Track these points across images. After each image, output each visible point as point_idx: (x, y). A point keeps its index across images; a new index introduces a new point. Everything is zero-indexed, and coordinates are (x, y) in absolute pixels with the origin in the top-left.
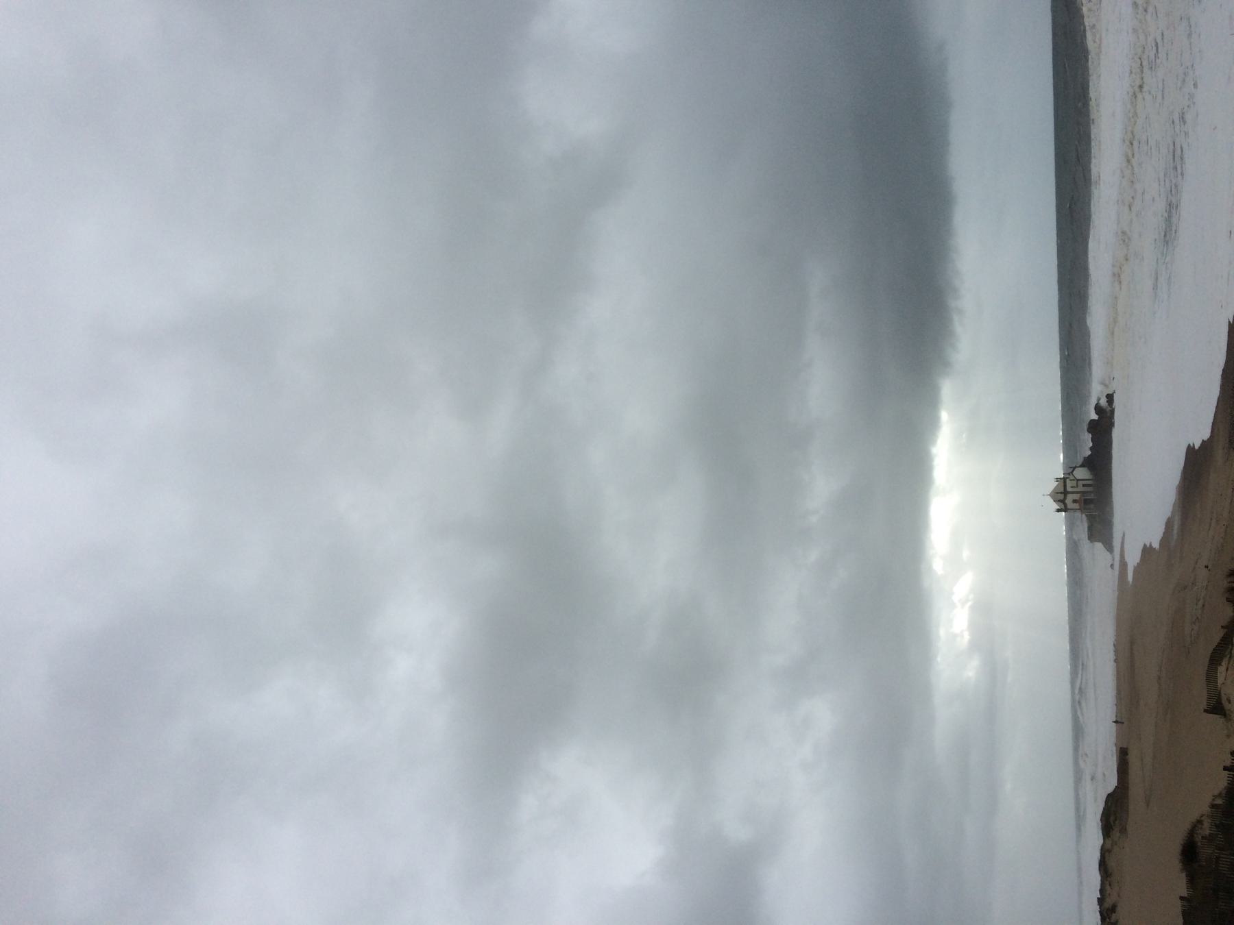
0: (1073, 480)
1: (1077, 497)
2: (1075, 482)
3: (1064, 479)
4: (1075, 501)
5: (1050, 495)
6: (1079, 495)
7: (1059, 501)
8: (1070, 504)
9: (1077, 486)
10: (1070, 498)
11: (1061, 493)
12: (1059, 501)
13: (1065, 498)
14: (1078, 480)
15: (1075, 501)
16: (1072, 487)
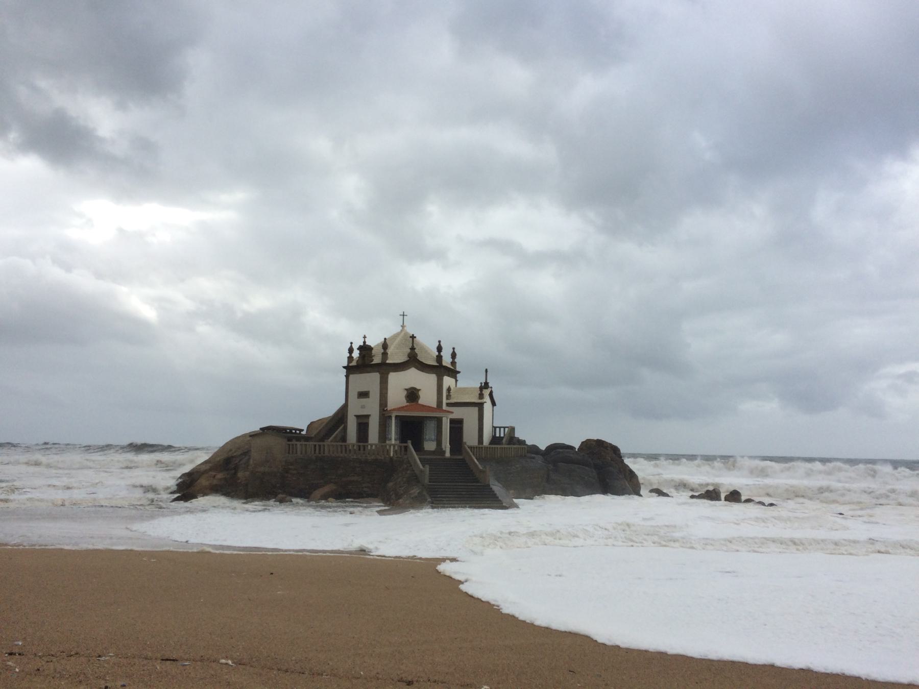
0: (481, 396)
1: (428, 397)
2: (477, 400)
3: (453, 372)
4: (412, 395)
6: (434, 405)
7: (413, 349)
8: (399, 382)
9: (448, 405)
10: (425, 383)
11: (439, 358)
12: (413, 349)
13: (424, 367)
14: (480, 406)
15: (412, 395)
16: (449, 390)
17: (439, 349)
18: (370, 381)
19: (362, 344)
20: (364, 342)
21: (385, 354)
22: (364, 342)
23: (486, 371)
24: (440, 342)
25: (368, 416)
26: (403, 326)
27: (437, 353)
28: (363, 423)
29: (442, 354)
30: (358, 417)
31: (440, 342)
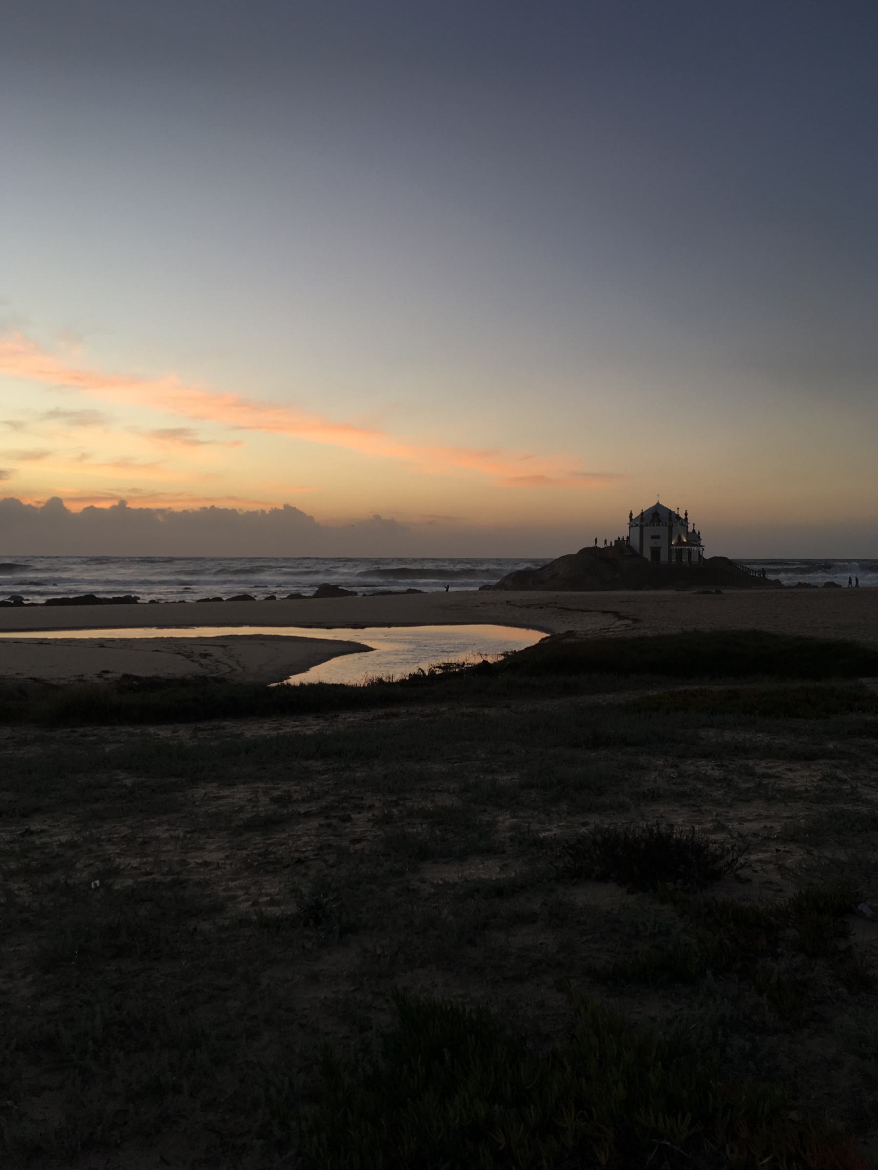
5: (658, 502)
12: (678, 515)
17: (686, 514)
18: (662, 531)
19: (654, 512)
20: (656, 511)
21: (670, 519)
22: (656, 511)
23: (694, 524)
24: (686, 511)
25: (660, 548)
26: (658, 501)
27: (685, 517)
28: (656, 552)
29: (688, 517)
30: (651, 548)
31: (686, 511)
